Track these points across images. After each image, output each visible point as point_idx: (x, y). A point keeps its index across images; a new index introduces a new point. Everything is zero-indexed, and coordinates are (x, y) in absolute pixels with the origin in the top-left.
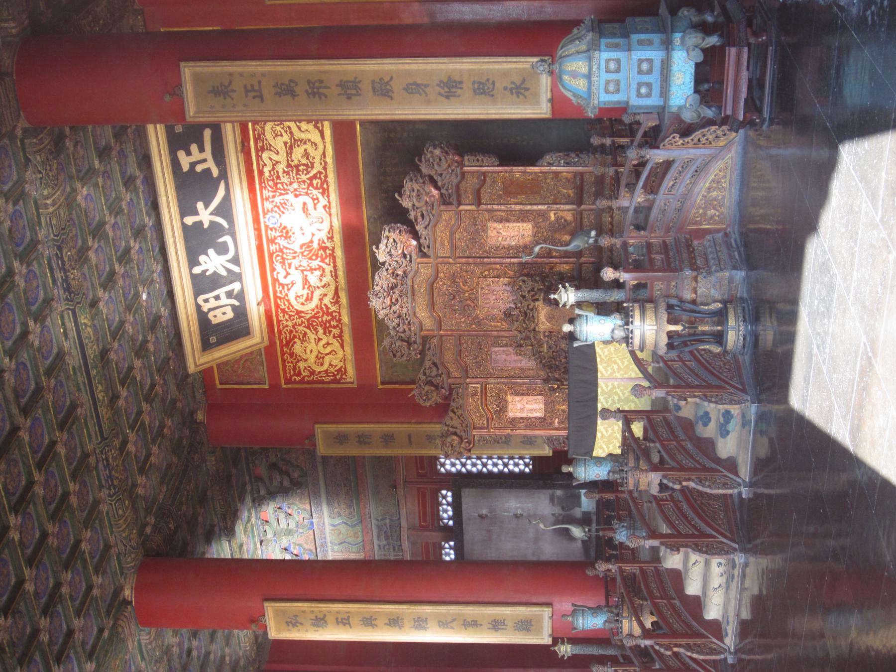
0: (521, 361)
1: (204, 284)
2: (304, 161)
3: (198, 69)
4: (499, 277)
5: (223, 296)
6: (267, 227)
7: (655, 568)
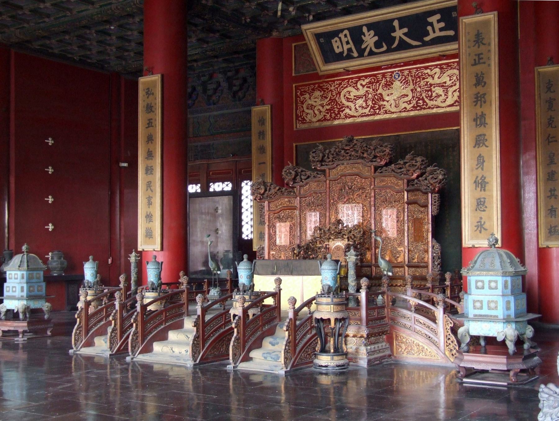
0: (311, 230)
1: (356, 34)
2: (434, 94)
3: (493, 22)
4: (363, 216)
5: (349, 46)
6: (393, 72)
7: (184, 313)
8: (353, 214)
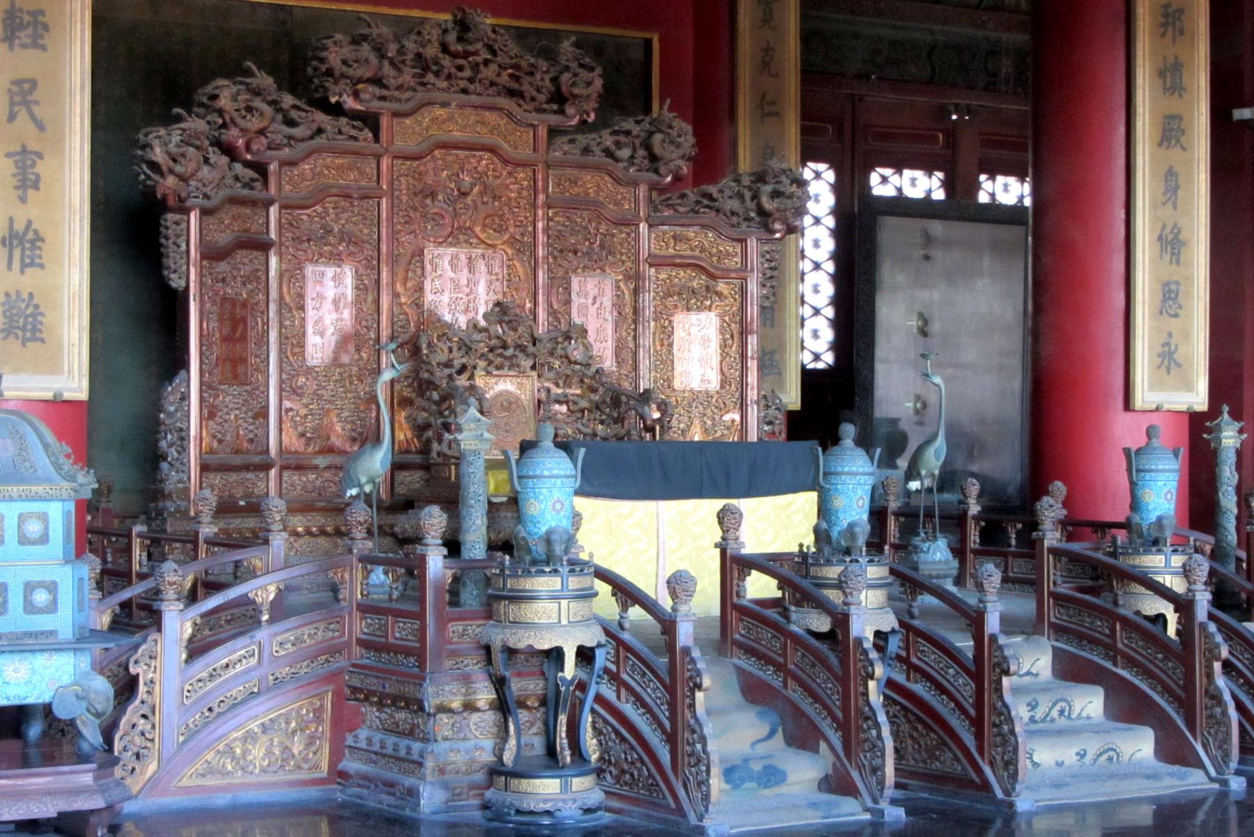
8: (472, 283)
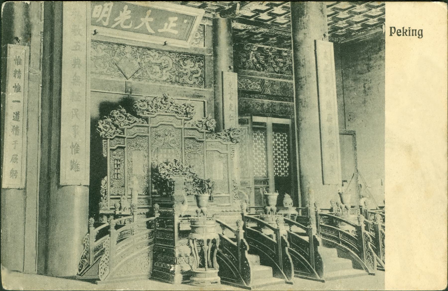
5: (105, 16)
